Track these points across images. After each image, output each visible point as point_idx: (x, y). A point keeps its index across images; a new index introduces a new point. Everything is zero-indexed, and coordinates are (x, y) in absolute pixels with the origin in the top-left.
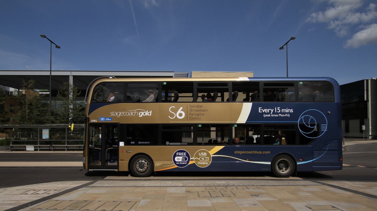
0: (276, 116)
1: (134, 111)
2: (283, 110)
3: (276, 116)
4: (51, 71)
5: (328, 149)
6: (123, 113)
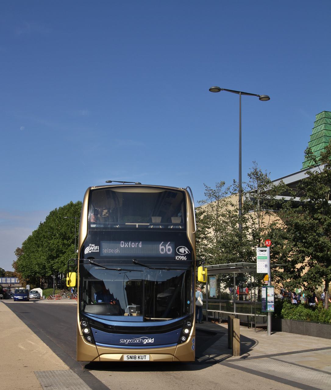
6: (131, 341)
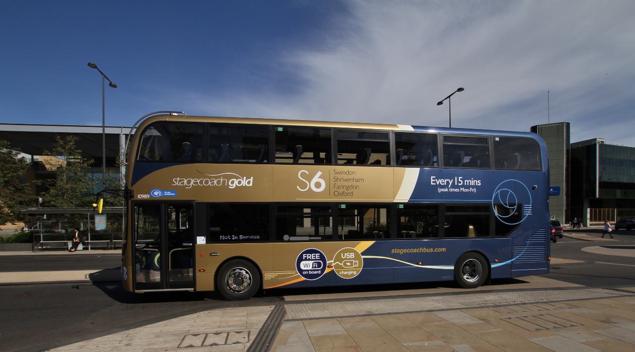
0: (456, 190)
1: (219, 177)
2: (467, 182)
3: (456, 190)
4: (103, 127)
5: (530, 243)
6: (198, 181)
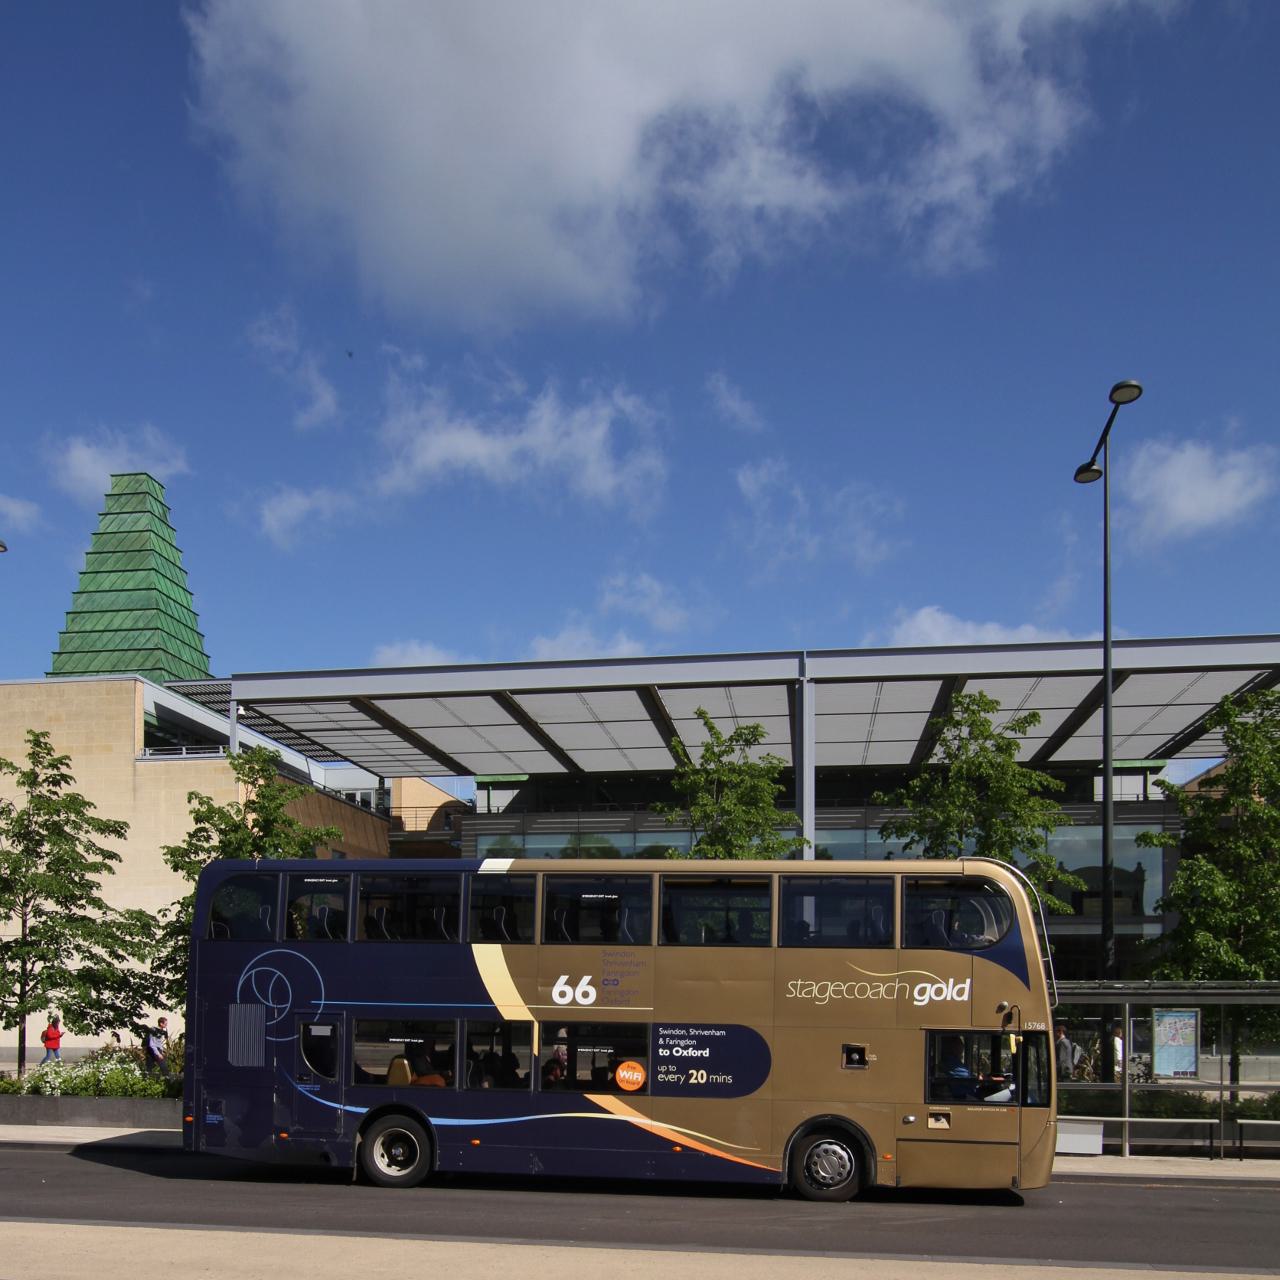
1: (892, 979)
6: (844, 988)
